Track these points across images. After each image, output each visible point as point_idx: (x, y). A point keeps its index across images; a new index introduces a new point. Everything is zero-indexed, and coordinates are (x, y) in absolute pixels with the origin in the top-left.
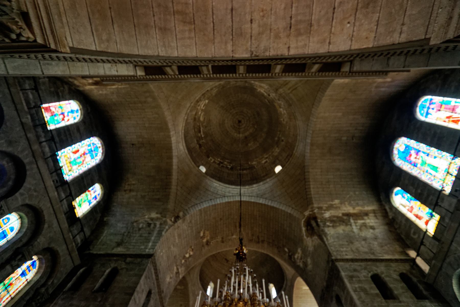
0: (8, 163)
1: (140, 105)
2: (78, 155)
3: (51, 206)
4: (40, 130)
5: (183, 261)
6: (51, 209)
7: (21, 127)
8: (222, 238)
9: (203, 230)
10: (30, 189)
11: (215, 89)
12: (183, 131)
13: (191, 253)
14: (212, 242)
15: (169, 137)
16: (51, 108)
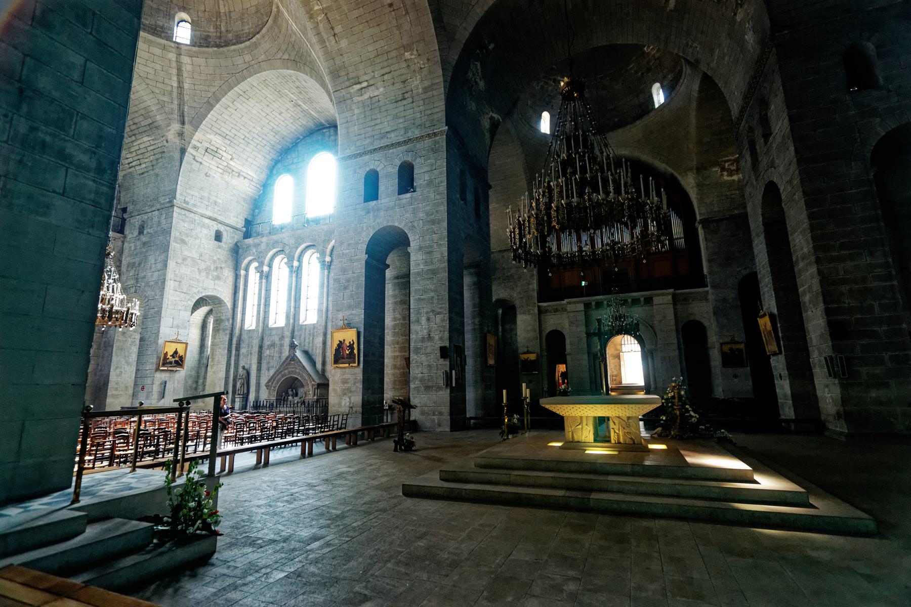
11: (631, 69)
12: (682, 81)
15: (701, 91)
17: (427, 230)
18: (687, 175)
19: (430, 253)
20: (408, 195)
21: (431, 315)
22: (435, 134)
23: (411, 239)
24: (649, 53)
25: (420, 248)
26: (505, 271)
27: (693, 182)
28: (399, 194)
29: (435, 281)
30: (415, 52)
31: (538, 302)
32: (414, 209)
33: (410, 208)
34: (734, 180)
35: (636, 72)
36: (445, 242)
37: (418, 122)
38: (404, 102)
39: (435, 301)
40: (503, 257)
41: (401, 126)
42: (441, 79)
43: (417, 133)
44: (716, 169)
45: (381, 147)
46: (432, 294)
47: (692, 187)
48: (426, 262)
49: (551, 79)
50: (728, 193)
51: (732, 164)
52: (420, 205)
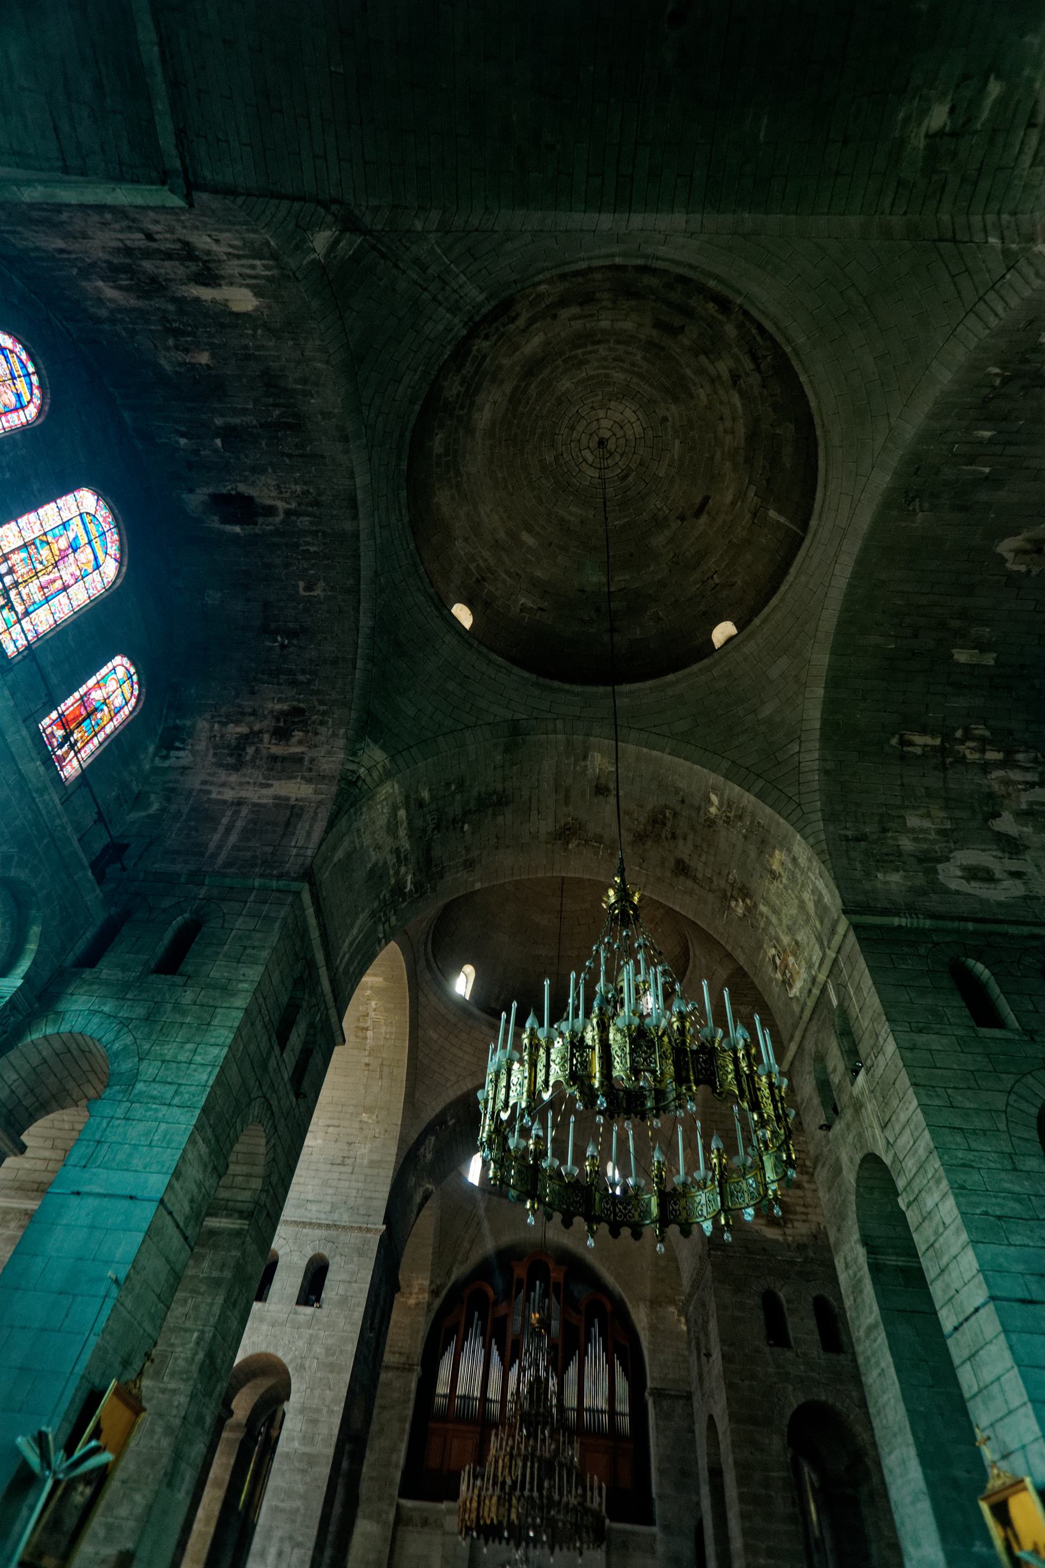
17: (321, 1379)
19: (314, 1422)
20: (308, 1310)
21: (287, 1548)
22: (368, 1230)
23: (294, 1387)
25: (303, 1410)
28: (298, 1303)
29: (308, 1479)
30: (374, 1117)
31: (401, 1495)
32: (311, 1335)
33: (307, 1332)
36: (339, 1409)
37: (351, 1202)
38: (342, 1169)
39: (299, 1519)
41: (329, 1199)
42: (394, 1159)
43: (345, 1219)
45: (295, 1222)
46: (299, 1503)
48: (304, 1437)
52: (322, 1333)
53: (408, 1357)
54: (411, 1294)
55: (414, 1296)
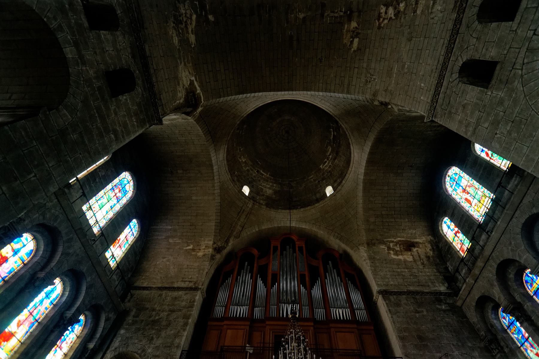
0: (510, 274)
1: (383, 213)
2: (468, 197)
3: (515, 216)
4: (477, 251)
5: (402, 6)
6: (516, 215)
7: (478, 280)
8: (322, 15)
9: (352, 50)
10: (512, 250)
11: (311, 178)
12: (350, 169)
13: (383, 10)
14: (342, 14)
15: (366, 174)
16: (460, 248)
18: (359, 249)
24: (324, 169)
26: (154, 313)
27: (365, 255)
34: (400, 260)
35: (315, 180)
40: (160, 295)
44: (383, 247)
47: (365, 260)
49: (255, 170)
50: (399, 270)
51: (396, 245)
53: (195, 284)
54: (200, 250)
55: (202, 251)
